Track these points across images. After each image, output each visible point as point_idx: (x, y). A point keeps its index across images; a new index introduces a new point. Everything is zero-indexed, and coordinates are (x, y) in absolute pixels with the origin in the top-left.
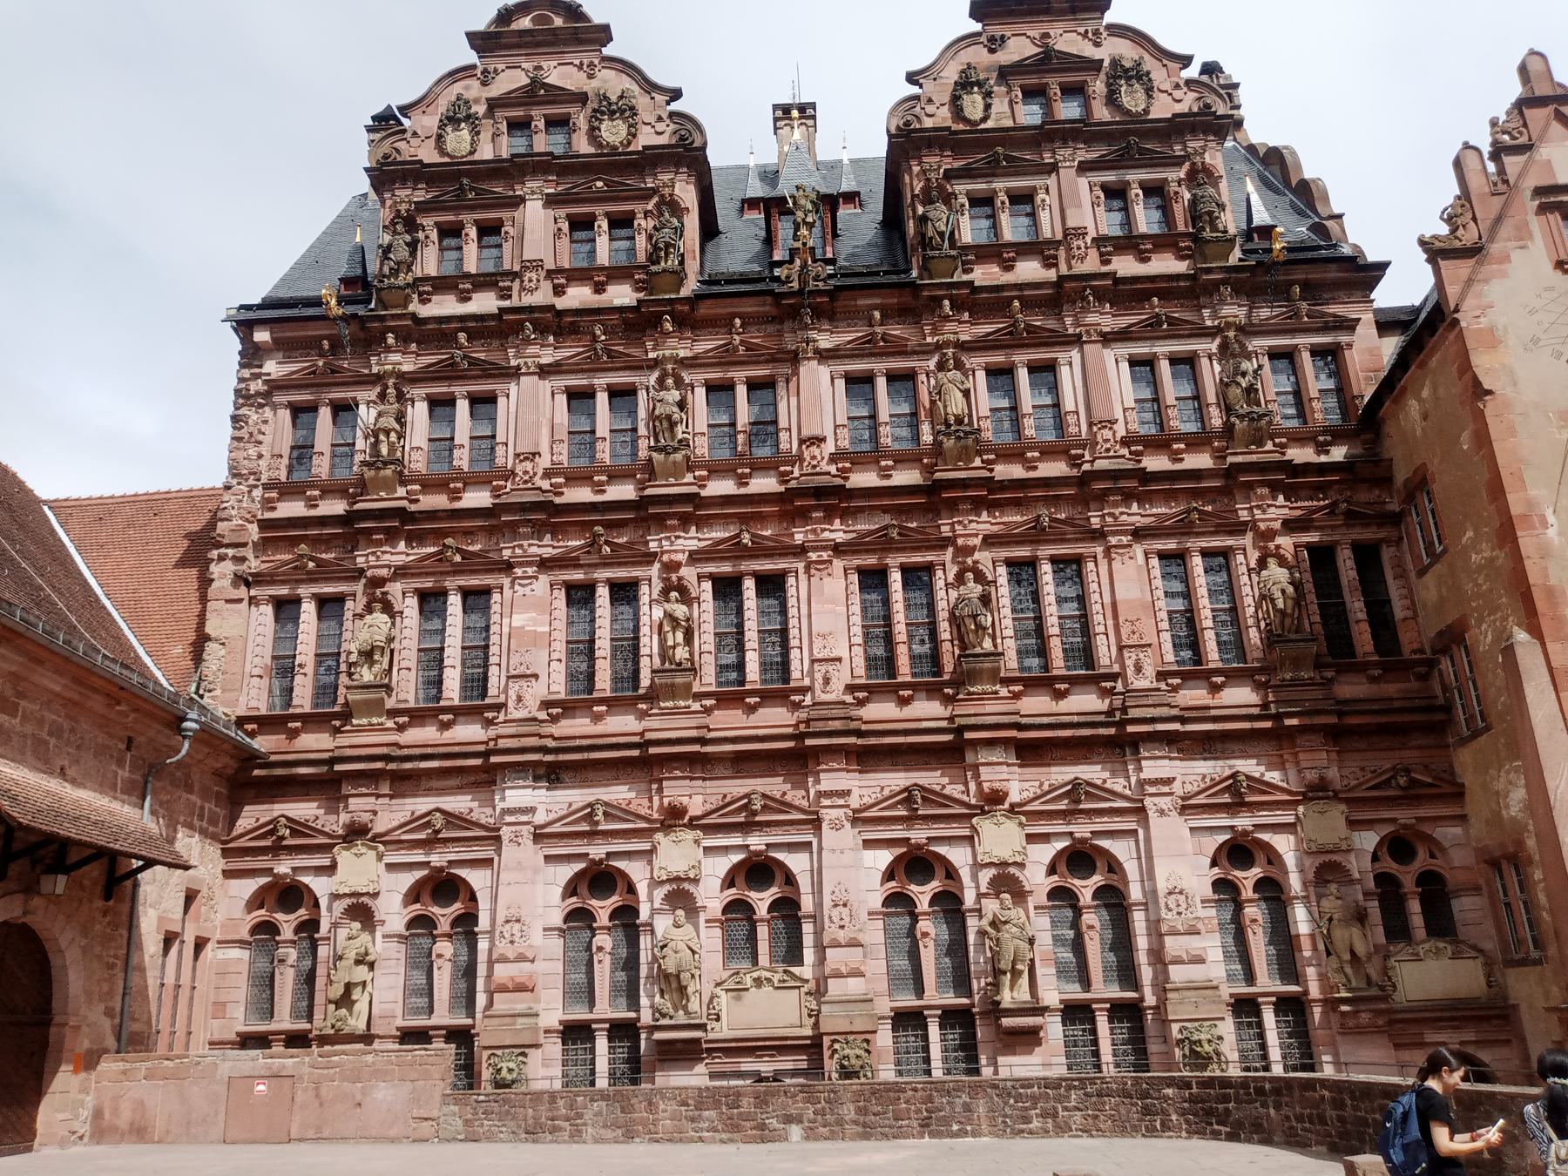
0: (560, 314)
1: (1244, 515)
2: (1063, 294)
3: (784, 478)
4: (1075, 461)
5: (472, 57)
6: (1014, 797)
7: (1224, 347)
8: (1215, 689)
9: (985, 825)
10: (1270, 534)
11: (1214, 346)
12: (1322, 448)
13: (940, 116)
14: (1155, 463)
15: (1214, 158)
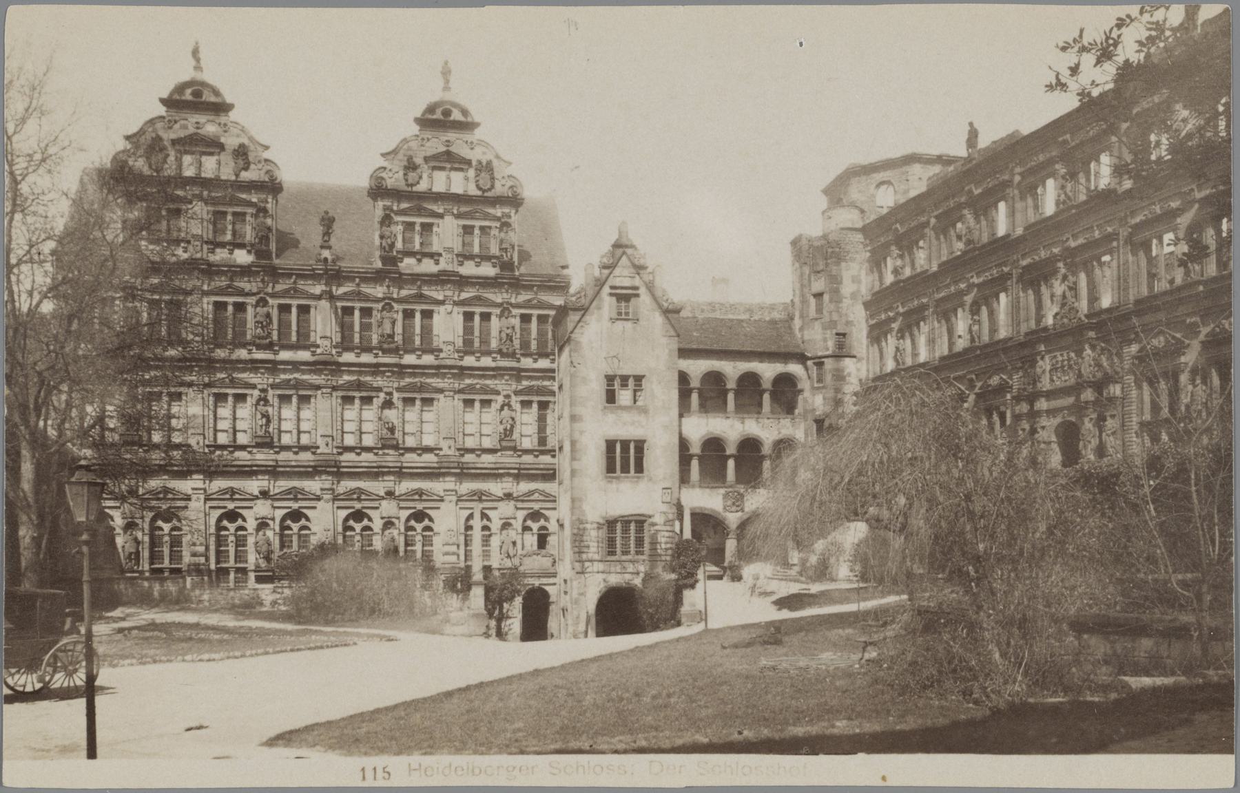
0: (210, 265)
1: (499, 388)
2: (441, 279)
3: (314, 354)
4: (437, 358)
5: (162, 110)
6: (397, 494)
7: (502, 312)
8: (479, 456)
9: (384, 503)
10: (508, 396)
11: (498, 311)
12: (535, 361)
13: (395, 179)
14: (469, 361)
15: (514, 219)
